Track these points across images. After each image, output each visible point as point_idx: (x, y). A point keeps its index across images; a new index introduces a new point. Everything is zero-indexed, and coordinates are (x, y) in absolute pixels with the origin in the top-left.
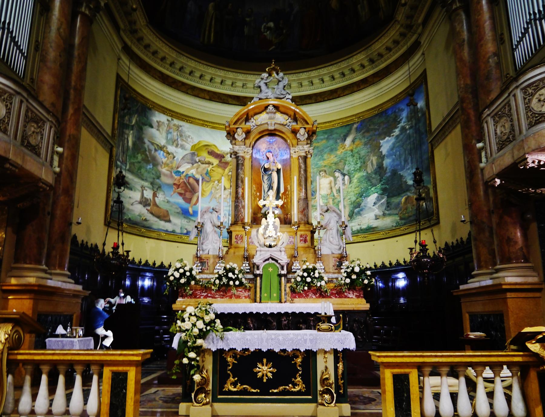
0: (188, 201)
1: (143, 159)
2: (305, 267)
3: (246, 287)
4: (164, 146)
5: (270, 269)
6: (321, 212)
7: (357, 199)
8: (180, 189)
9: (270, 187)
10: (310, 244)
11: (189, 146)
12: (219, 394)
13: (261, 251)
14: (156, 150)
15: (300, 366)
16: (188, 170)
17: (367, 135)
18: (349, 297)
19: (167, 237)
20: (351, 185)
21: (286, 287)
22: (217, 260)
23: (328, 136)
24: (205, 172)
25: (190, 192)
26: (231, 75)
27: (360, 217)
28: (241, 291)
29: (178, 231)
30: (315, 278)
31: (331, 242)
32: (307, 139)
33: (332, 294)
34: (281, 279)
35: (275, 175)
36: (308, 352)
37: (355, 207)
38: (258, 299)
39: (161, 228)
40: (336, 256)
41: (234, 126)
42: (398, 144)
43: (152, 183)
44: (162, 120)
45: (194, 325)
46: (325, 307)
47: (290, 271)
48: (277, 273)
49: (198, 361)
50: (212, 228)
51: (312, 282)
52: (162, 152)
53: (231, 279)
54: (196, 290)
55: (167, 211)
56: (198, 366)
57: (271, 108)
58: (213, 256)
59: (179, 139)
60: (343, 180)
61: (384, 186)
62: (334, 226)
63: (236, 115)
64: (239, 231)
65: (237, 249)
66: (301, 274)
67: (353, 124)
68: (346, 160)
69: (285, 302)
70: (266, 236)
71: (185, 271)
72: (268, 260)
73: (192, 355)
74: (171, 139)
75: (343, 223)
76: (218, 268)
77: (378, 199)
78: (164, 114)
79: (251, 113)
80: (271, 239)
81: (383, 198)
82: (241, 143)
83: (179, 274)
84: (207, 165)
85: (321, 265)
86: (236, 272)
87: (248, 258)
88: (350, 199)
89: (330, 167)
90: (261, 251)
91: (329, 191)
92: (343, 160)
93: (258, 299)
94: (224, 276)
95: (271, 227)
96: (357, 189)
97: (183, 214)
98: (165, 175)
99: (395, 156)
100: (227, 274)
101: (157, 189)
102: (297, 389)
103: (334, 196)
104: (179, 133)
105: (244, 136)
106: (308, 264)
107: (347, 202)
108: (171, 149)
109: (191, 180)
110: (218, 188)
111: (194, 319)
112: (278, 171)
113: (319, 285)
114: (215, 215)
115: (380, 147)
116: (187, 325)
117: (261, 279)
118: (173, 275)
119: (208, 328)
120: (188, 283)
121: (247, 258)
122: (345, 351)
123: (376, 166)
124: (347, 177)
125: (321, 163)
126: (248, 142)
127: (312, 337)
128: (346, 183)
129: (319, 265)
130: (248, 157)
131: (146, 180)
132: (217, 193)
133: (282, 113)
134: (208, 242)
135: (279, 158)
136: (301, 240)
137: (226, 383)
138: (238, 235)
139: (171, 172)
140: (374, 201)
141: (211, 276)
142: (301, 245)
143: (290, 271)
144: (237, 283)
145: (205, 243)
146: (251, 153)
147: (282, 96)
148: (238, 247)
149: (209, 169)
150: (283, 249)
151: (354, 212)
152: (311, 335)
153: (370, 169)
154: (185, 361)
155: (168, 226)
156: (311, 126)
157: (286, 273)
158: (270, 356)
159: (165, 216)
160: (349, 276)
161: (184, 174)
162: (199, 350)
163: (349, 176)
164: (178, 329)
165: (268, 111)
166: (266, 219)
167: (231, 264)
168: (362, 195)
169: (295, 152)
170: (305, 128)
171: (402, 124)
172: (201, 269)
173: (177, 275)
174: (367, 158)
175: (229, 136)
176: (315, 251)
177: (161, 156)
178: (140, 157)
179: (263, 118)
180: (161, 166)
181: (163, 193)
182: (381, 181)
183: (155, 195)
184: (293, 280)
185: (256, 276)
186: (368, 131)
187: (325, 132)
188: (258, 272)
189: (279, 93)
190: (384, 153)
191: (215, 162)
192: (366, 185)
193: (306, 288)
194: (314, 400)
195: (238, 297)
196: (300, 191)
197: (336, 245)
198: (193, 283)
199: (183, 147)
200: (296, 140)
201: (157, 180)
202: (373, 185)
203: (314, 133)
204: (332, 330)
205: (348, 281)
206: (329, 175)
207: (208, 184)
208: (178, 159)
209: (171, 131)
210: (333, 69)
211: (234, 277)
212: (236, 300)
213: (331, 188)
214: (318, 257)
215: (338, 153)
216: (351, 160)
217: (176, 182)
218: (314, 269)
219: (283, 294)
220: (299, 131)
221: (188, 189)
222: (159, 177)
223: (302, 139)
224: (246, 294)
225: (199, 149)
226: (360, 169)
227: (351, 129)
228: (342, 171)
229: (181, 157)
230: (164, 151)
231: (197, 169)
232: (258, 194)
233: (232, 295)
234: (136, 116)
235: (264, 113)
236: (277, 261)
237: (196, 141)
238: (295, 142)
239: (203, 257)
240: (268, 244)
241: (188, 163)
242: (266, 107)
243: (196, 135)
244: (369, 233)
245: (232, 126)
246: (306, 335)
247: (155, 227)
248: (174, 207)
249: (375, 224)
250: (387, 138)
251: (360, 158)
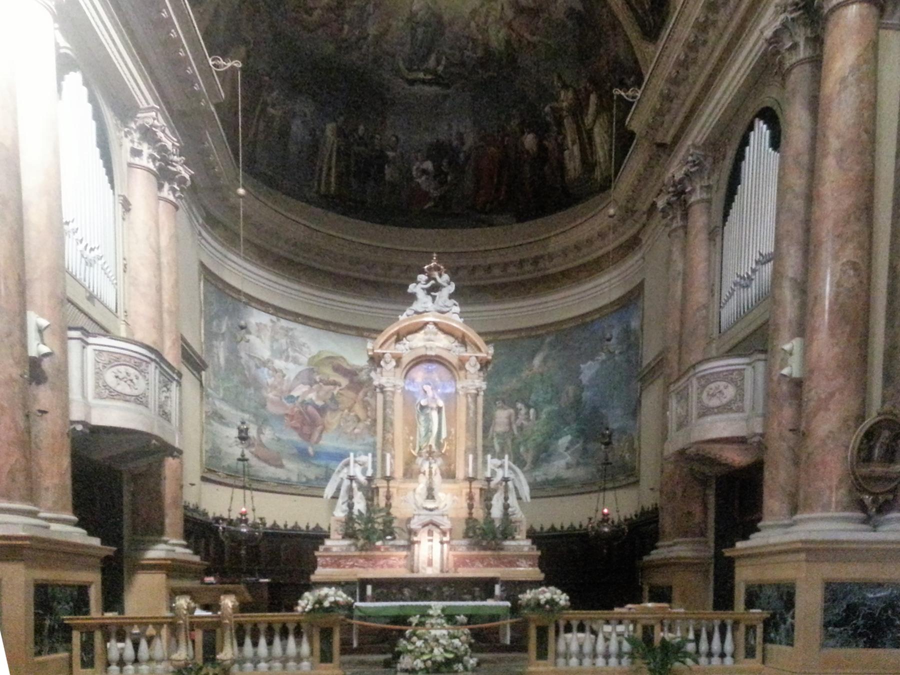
11: (304, 359)
16: (305, 393)
44: (264, 322)
60: (528, 413)
107: (531, 444)
108: (279, 364)
124: (532, 411)
149: (335, 392)
161: (300, 400)
163: (536, 409)
168: (553, 435)
199: (296, 361)
216: (540, 387)
226: (550, 402)
227: (542, 343)
250: (589, 363)
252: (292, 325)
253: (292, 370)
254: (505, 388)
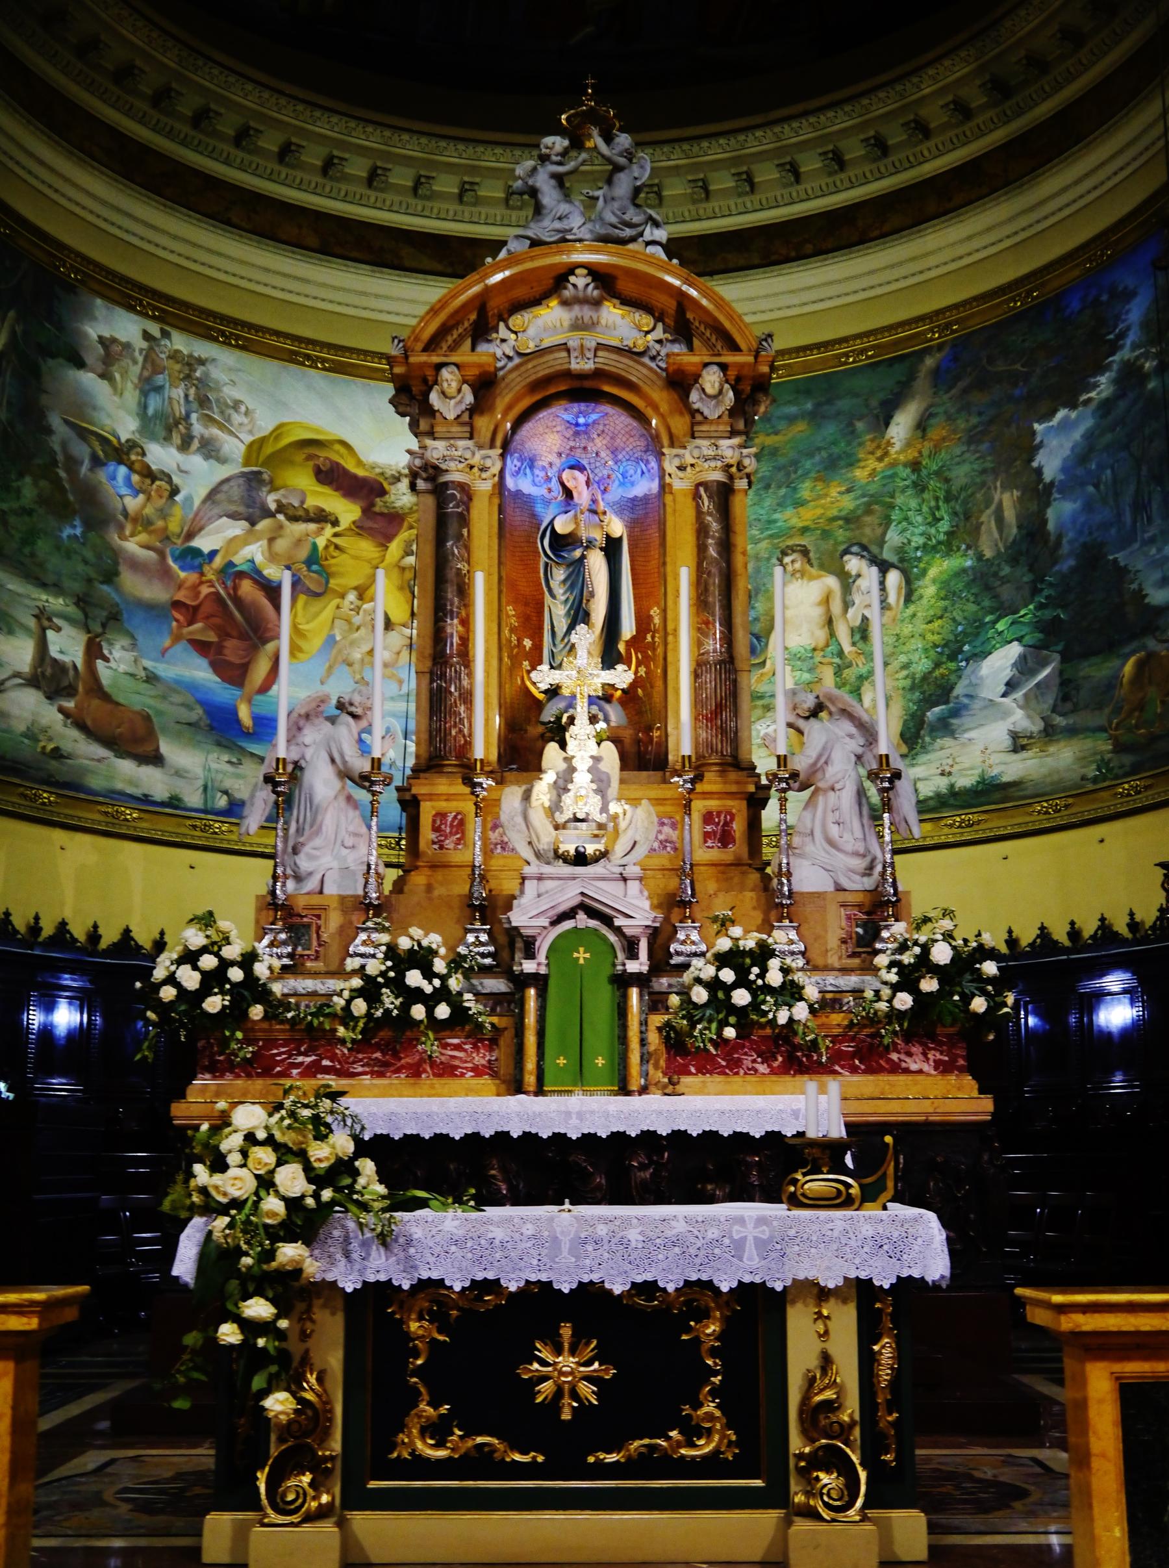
1: (42, 500)
2: (724, 944)
3: (480, 1026)
4: (132, 445)
5: (582, 955)
6: (792, 719)
7: (937, 665)
8: (199, 625)
9: (579, 615)
10: (744, 852)
11: (234, 447)
12: (371, 1473)
13: (540, 878)
14: (97, 462)
15: (714, 1352)
16: (234, 543)
17: (979, 398)
18: (907, 1071)
19: (146, 827)
20: (912, 608)
21: (644, 1027)
22: (357, 918)
23: (818, 405)
24: (303, 553)
25: (243, 636)
26: (411, 147)
27: (947, 741)
28: (457, 1047)
29: (194, 799)
30: (768, 989)
31: (831, 842)
32: (733, 412)
33: (837, 1057)
34: (625, 997)
35: (597, 563)
36: (748, 1292)
37: (929, 702)
38: (530, 1079)
39: (119, 786)
40: (850, 898)
41: (423, 358)
42: (1109, 437)
43: (82, 601)
44: (123, 337)
45: (266, 1183)
46: (810, 1108)
47: (661, 963)
48: (607, 971)
49: (281, 1335)
50: (336, 784)
51: (755, 1005)
52: (122, 470)
53: (416, 995)
54: (271, 1043)
55: (147, 718)
56: (283, 1357)
57: (580, 280)
58: (342, 898)
59: (194, 416)
61: (1048, 614)
62: (843, 771)
63: (434, 311)
64: (449, 797)
65: (439, 875)
66: (709, 972)
67: (921, 355)
68: (892, 507)
69: (644, 1090)
70: (560, 818)
71: (225, 964)
72: (569, 914)
73: (258, 1308)
74: (160, 415)
75: (884, 760)
76: (362, 950)
77: (1024, 667)
78: (131, 308)
79: (496, 304)
80: (581, 825)
81: (1043, 664)
82: (456, 429)
83: (197, 976)
84: (312, 527)
85: (793, 935)
86: (439, 966)
87: (488, 909)
88: (906, 666)
89: (826, 534)
90: (540, 878)
91: (821, 635)
92: (879, 505)
93: (530, 1079)
94: (389, 983)
95: (582, 778)
96: (937, 624)
97: (212, 728)
98: (136, 565)
99: (1096, 486)
100: (401, 976)
101: (104, 626)
102: (705, 1447)
103: (841, 653)
104: (192, 391)
105: (469, 398)
106: (736, 931)
108: (161, 456)
109: (247, 588)
110: (357, 620)
111: (265, 1156)
112: (611, 548)
113: (782, 1017)
114: (346, 731)
115: (1033, 450)
116: (236, 1183)
117: (542, 995)
118: (171, 980)
119: (327, 1194)
120: (235, 1014)
121: (481, 908)
122: (907, 1287)
123: (1015, 531)
124: (894, 578)
125: (790, 518)
126: (484, 424)
127: (764, 1232)
128: (892, 599)
129: (782, 937)
130: (484, 486)
131: (56, 588)
132: (353, 643)
133: (627, 302)
134: (317, 842)
135: (616, 493)
136: (707, 836)
137: (401, 1427)
138: (442, 815)
139: (161, 554)
140: (1007, 674)
141: (334, 984)
142: (705, 854)
143: (661, 963)
144: (443, 1011)
145: (307, 849)
146: (496, 469)
147: (628, 232)
148: (446, 866)
149: (321, 542)
150: (633, 870)
151: (922, 722)
152: (761, 1221)
154: (229, 1333)
155: (152, 781)
156: (751, 359)
157: (645, 969)
158: (588, 1310)
159: (137, 740)
160: (908, 980)
161: (218, 562)
162: (289, 1289)
163: (905, 573)
164: (196, 1198)
165: (568, 293)
166: (563, 745)
167: (416, 932)
169: (682, 468)
170: (723, 367)
171: (1125, 354)
172: (291, 956)
173: (190, 979)
174: (979, 496)
175: (404, 399)
176: (766, 879)
177: (118, 487)
178: (29, 490)
179: (546, 323)
180: (121, 528)
181: (126, 642)
182: (1035, 591)
183: (94, 651)
184: (674, 1000)
185: (521, 981)
186: (981, 384)
187: (804, 389)
188: (529, 967)
189: (614, 220)
190: (1049, 475)
191: (348, 512)
192: (972, 607)
193: (730, 1033)
194: (774, 1496)
195: (447, 1070)
196: (701, 629)
197: (856, 854)
198: (257, 1012)
199: (209, 450)
200: (687, 418)
201: (105, 588)
202: (1003, 609)
203: (761, 385)
204: (847, 1202)
205: (904, 1001)
206: (822, 567)
207: (316, 605)
208: (189, 499)
209: (160, 379)
210: (838, 122)
211: (428, 989)
212: (436, 1081)
213: (830, 622)
214: (778, 904)
215: (860, 474)
216: (913, 504)
217: (181, 596)
218: (764, 954)
219: (635, 1058)
220: (697, 377)
221: (235, 626)
222: (110, 577)
223: (711, 411)
224: (480, 1058)
225: (281, 458)
226: (948, 546)
227: (912, 377)
228: (874, 549)
229: (203, 492)
230: (131, 467)
231: (271, 540)
232: (528, 643)
233: (422, 1061)
234: (12, 314)
235: (554, 303)
236: (607, 920)
237: (265, 424)
238: (679, 424)
239: (300, 903)
240: (570, 848)
241: (234, 516)
242: (562, 277)
243: (272, 402)
244: (985, 810)
245: (417, 358)
246: (741, 1221)
247: (96, 783)
248: (177, 699)
249: (1012, 768)
250: (1061, 414)
251: (947, 500)
252: (202, 348)
253: (197, 476)
254: (807, 516)
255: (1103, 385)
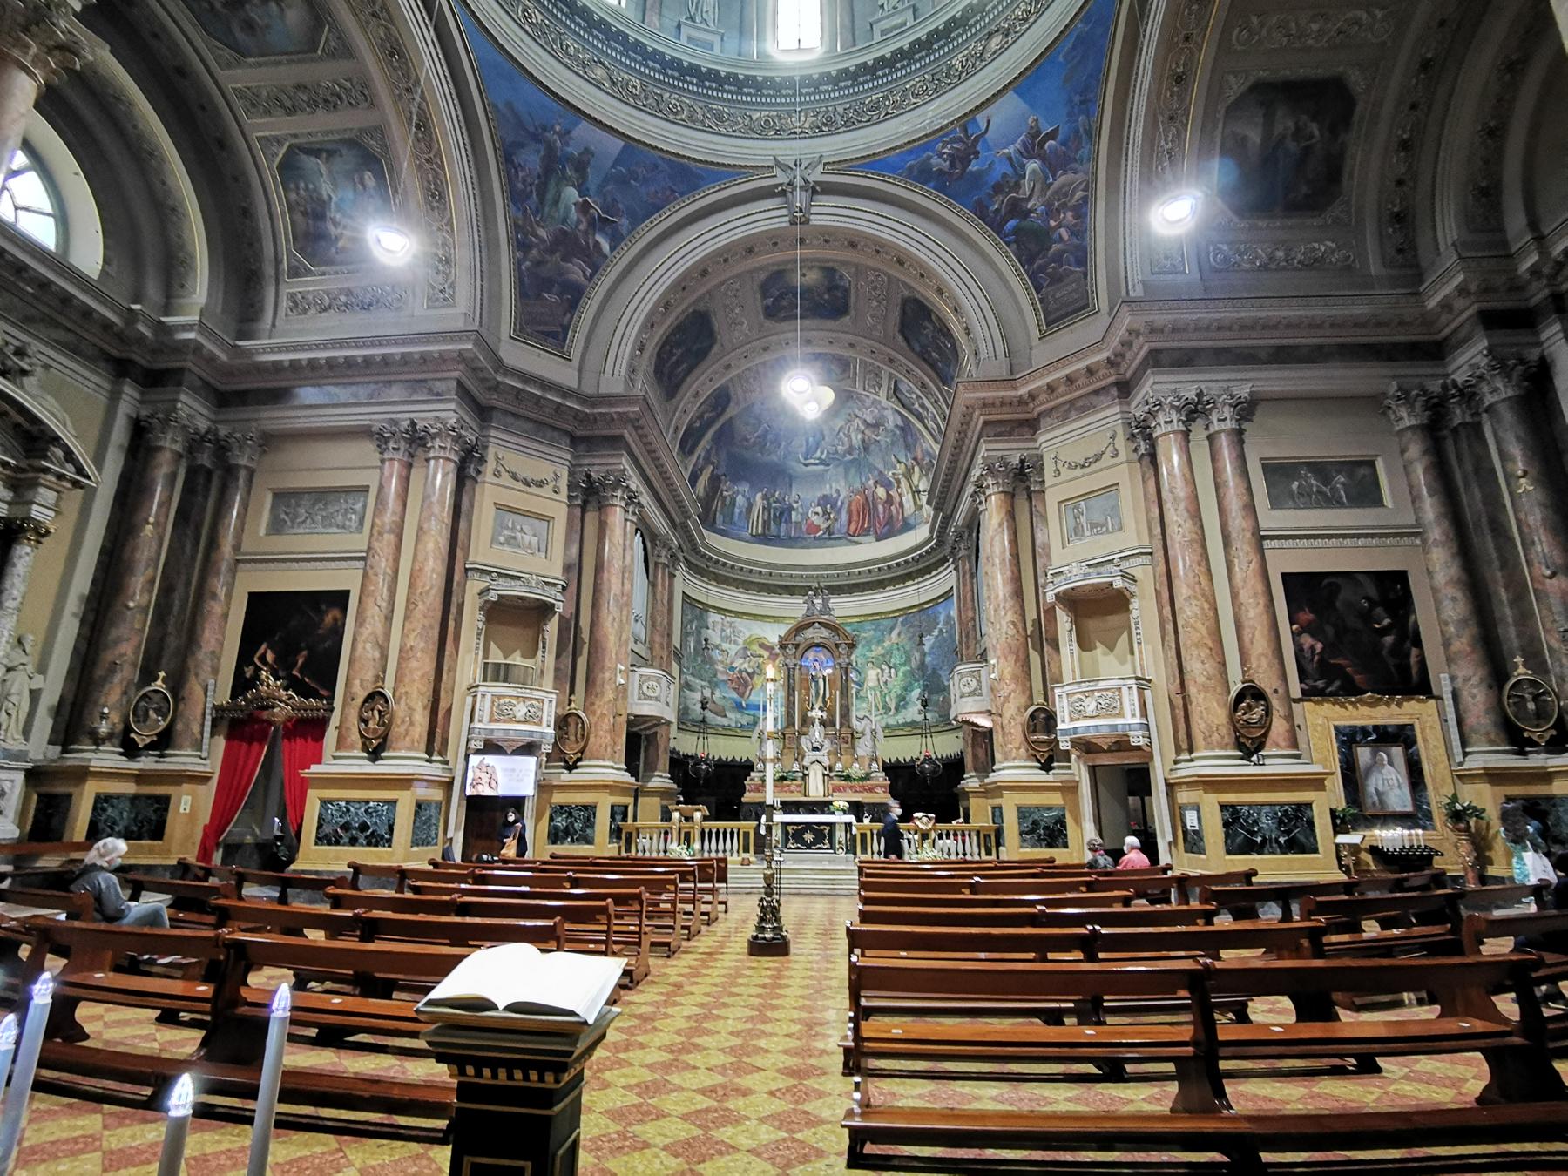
0: (742, 695)
9: (817, 693)
11: (740, 641)
62: (868, 732)
92: (889, 652)
107: (893, 695)
153: (914, 664)
155: (725, 722)
168: (907, 688)
177: (717, 655)
179: (809, 633)
191: (766, 654)
199: (736, 643)
221: (743, 683)
225: (751, 643)
226: (904, 664)
253: (733, 649)
255: (936, 633)
